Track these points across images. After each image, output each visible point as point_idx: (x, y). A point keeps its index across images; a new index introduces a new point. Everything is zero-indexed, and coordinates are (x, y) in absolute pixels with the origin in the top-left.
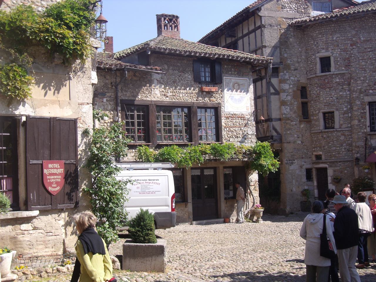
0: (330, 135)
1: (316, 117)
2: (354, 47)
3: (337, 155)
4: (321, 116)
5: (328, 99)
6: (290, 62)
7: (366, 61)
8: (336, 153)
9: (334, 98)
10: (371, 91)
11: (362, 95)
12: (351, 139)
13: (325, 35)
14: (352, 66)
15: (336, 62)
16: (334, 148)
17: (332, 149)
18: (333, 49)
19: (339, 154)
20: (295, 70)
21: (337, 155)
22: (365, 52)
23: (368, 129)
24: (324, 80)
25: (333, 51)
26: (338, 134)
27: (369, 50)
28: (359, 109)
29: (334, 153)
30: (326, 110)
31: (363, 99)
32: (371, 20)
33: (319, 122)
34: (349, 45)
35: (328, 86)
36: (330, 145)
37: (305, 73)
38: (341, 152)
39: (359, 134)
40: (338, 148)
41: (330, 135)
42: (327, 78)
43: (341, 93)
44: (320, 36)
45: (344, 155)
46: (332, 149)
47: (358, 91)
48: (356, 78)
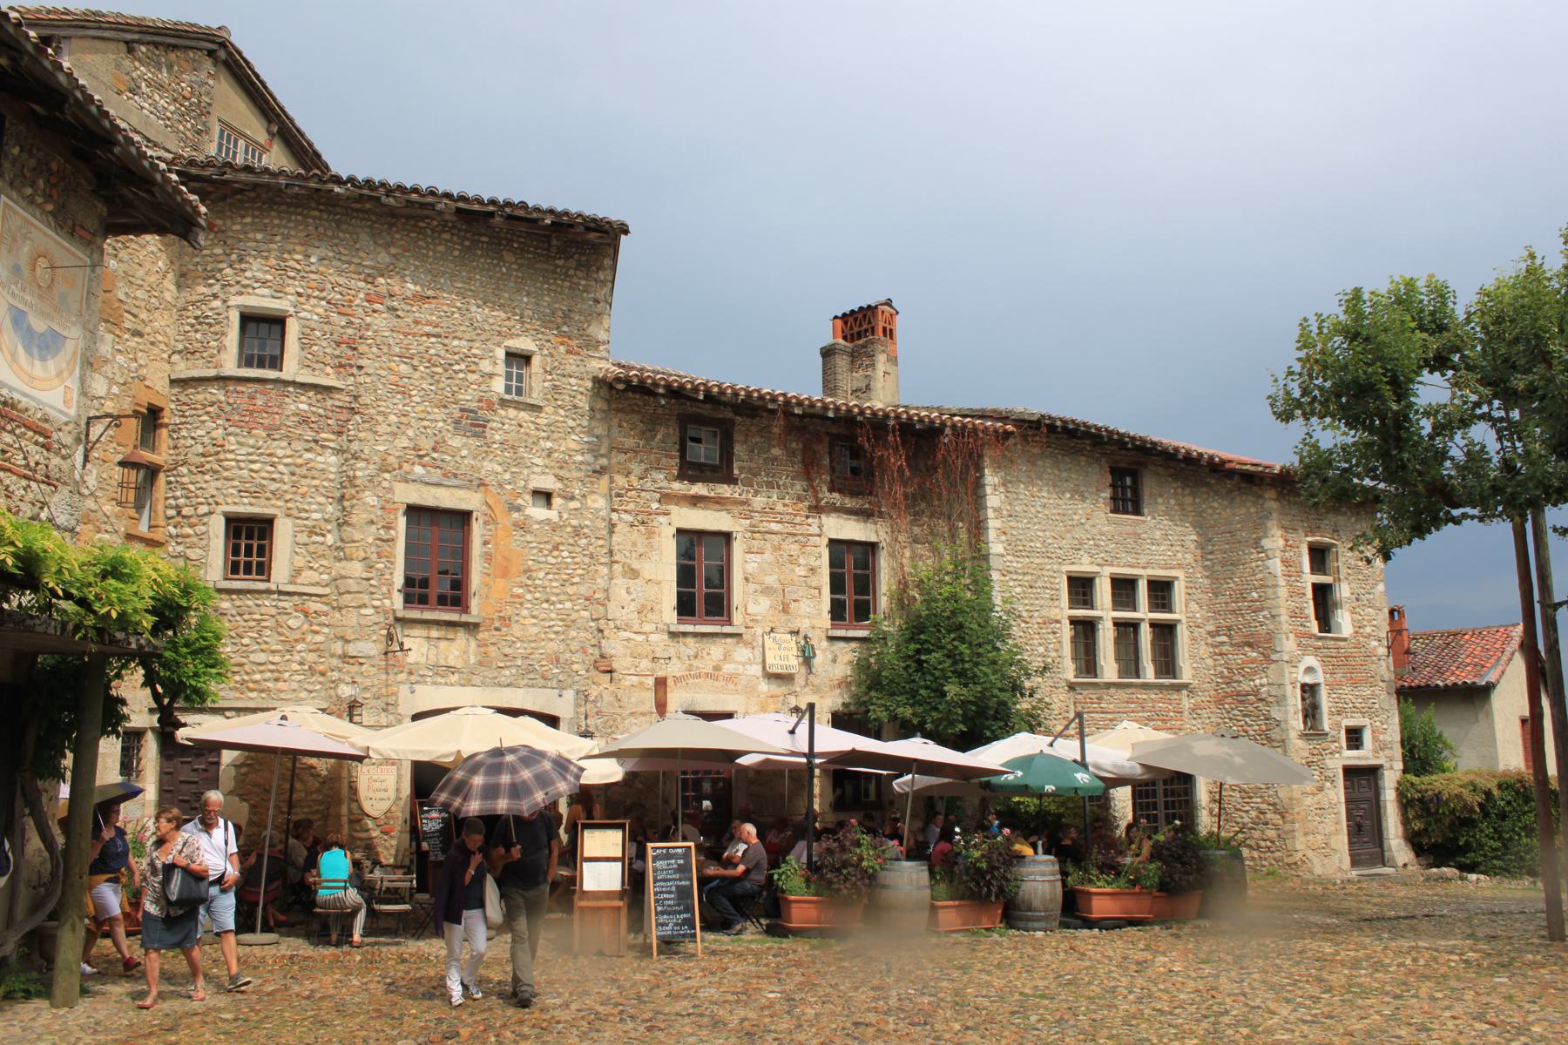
0: (250, 603)
1: (192, 526)
2: (377, 306)
3: (270, 685)
4: (218, 526)
5: (256, 467)
6: (123, 297)
7: (415, 362)
8: (268, 675)
9: (281, 468)
10: (419, 469)
11: (387, 475)
12: (326, 630)
13: (278, 238)
14: (360, 368)
15: (306, 341)
16: (262, 657)
17: (253, 657)
18: (300, 295)
19: (277, 680)
20: (137, 333)
21: (270, 685)
22: (414, 335)
23: (398, 600)
24: (252, 397)
25: (302, 300)
26: (281, 604)
27: (428, 329)
28: (372, 522)
29: (258, 677)
30: (246, 507)
31: (390, 490)
32: (447, 236)
33: (206, 548)
34: (362, 295)
35: (266, 422)
36: (246, 641)
37: (165, 356)
38: (286, 675)
39: (363, 611)
40: (277, 659)
41: (250, 603)
42: (262, 393)
43: (308, 455)
44: (259, 236)
45: (295, 686)
46: (253, 657)
47: (376, 459)
48: (373, 411)
